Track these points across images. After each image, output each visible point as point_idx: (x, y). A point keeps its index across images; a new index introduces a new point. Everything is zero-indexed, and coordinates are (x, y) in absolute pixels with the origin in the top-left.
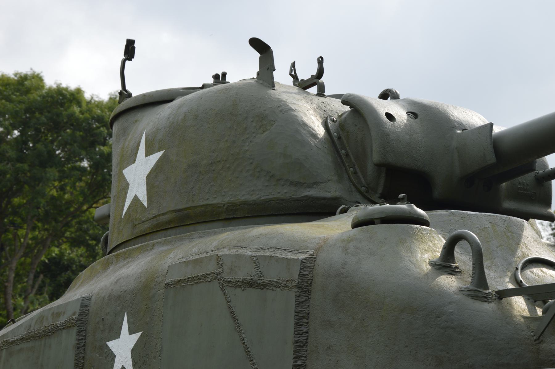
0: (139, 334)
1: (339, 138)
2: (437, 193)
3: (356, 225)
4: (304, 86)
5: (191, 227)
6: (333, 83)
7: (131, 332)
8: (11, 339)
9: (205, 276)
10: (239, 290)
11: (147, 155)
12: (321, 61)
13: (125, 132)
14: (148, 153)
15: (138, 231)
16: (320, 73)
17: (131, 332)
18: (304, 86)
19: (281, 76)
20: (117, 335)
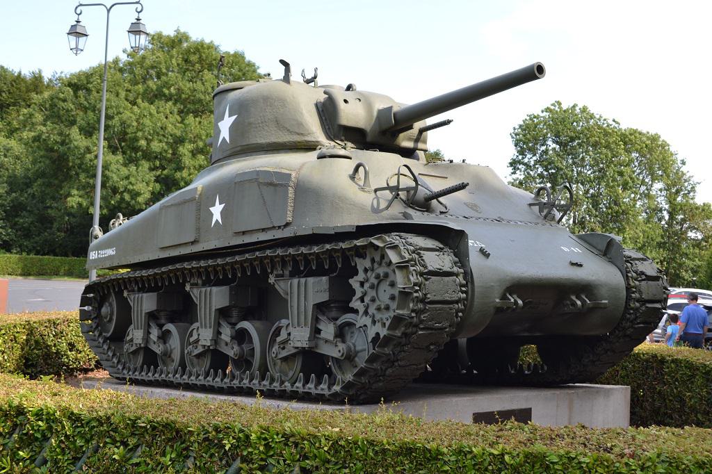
0: (224, 205)
1: (323, 111)
2: (369, 139)
3: (320, 157)
4: (308, 82)
5: (250, 154)
6: (320, 81)
7: (220, 204)
8: (167, 205)
9: (252, 180)
10: (265, 187)
11: (229, 116)
12: (316, 70)
13: (220, 103)
14: (229, 116)
15: (225, 155)
16: (315, 77)
17: (220, 204)
18: (308, 82)
19: (295, 76)
20: (214, 205)
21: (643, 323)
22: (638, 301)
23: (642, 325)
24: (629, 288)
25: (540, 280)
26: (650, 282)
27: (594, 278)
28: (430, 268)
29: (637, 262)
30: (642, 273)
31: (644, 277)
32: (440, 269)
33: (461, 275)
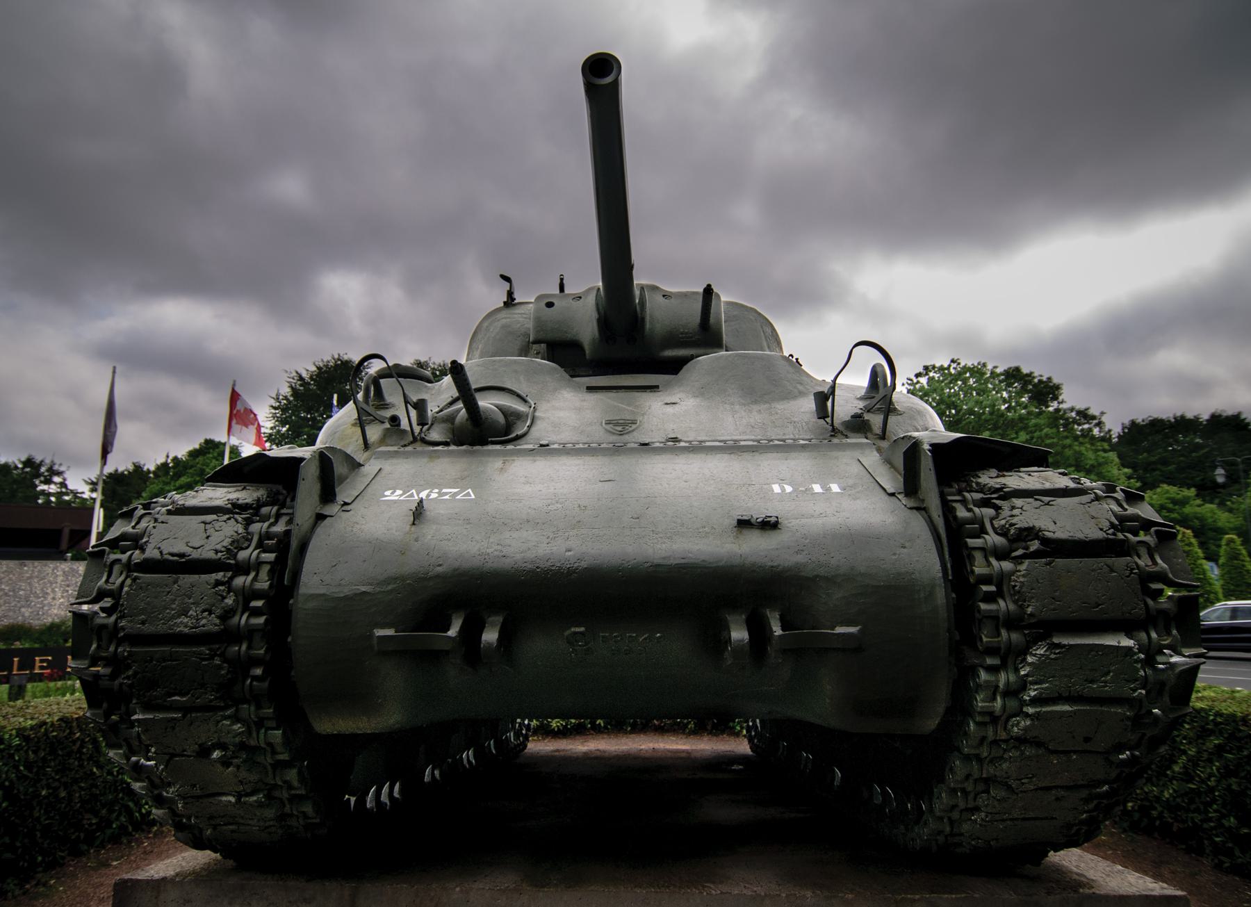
21: (1070, 699)
22: (1012, 622)
23: (1067, 708)
24: (960, 580)
25: (571, 571)
26: (1060, 562)
27: (800, 558)
28: (151, 553)
29: (1018, 502)
30: (1031, 533)
31: (1035, 545)
32: (182, 555)
33: (265, 569)
